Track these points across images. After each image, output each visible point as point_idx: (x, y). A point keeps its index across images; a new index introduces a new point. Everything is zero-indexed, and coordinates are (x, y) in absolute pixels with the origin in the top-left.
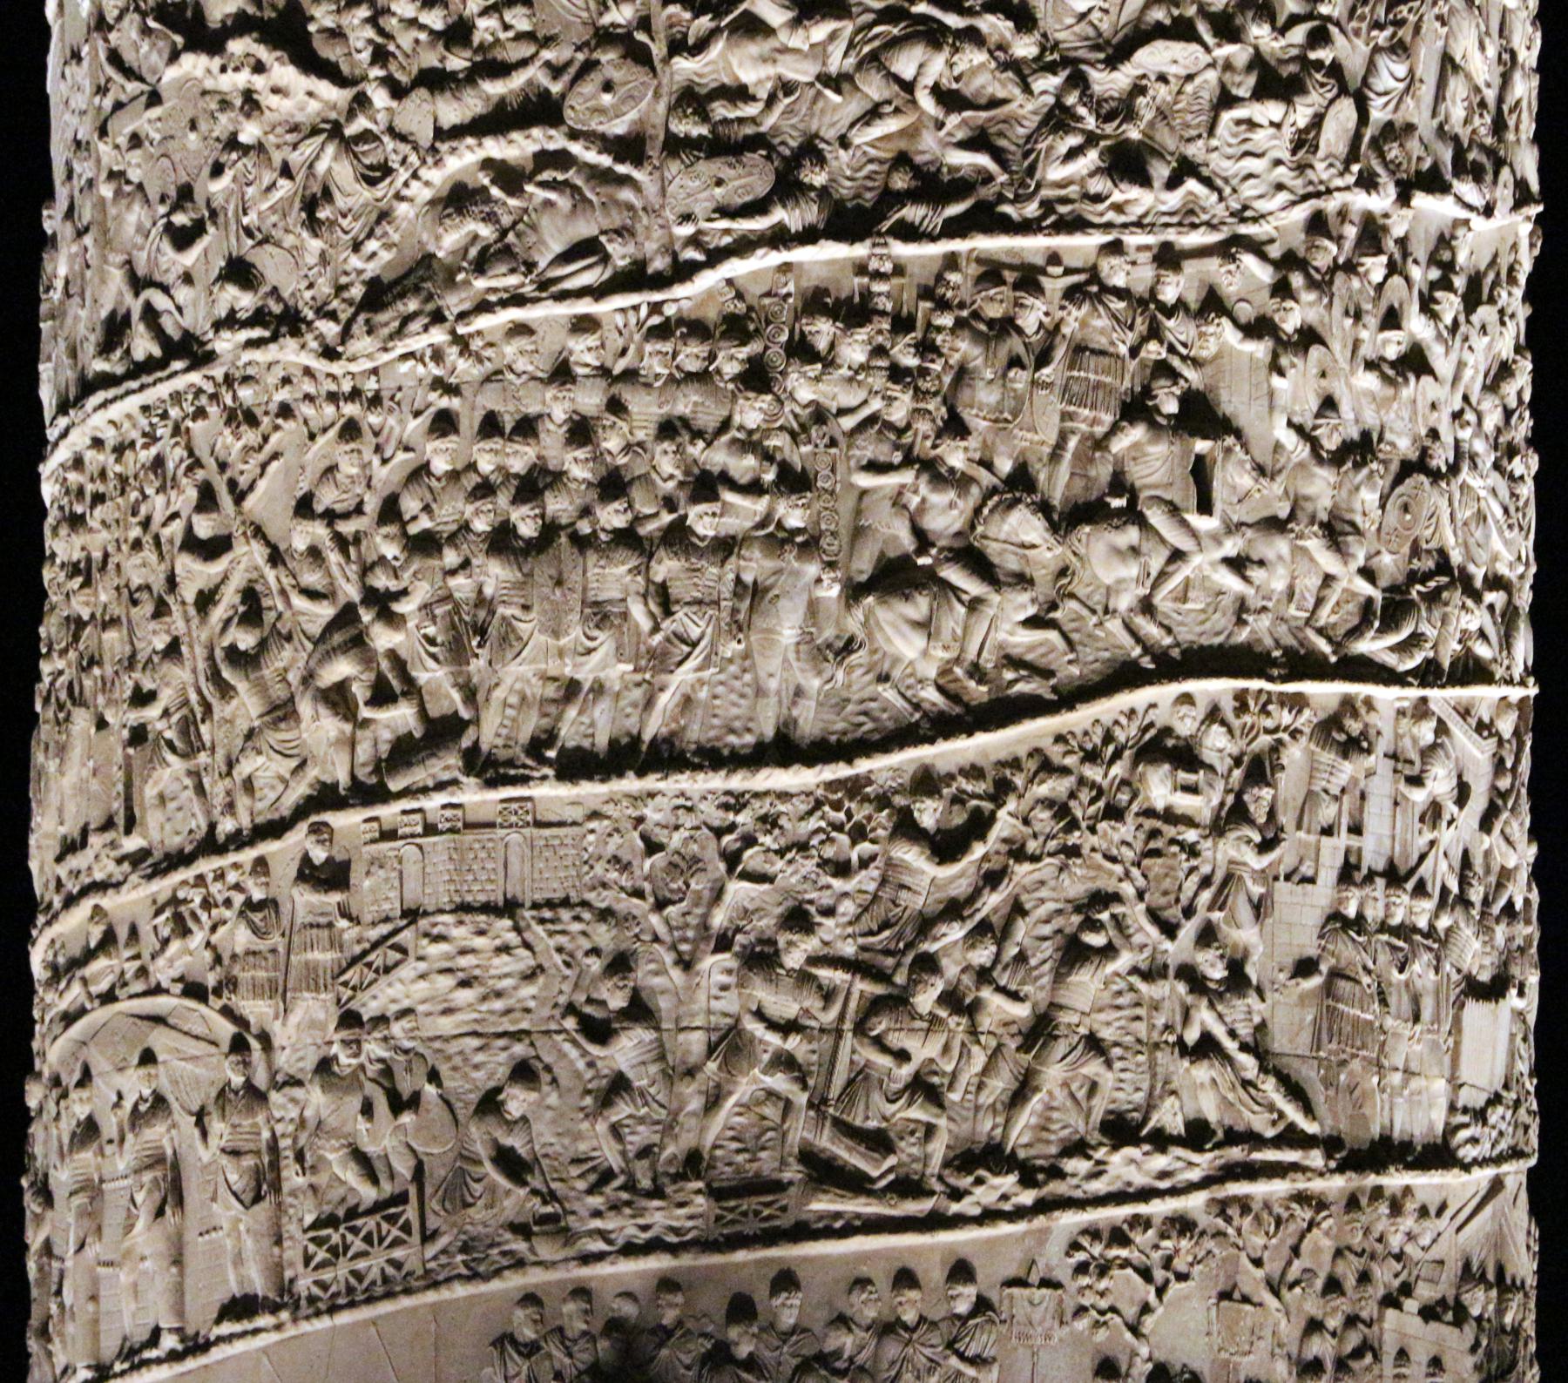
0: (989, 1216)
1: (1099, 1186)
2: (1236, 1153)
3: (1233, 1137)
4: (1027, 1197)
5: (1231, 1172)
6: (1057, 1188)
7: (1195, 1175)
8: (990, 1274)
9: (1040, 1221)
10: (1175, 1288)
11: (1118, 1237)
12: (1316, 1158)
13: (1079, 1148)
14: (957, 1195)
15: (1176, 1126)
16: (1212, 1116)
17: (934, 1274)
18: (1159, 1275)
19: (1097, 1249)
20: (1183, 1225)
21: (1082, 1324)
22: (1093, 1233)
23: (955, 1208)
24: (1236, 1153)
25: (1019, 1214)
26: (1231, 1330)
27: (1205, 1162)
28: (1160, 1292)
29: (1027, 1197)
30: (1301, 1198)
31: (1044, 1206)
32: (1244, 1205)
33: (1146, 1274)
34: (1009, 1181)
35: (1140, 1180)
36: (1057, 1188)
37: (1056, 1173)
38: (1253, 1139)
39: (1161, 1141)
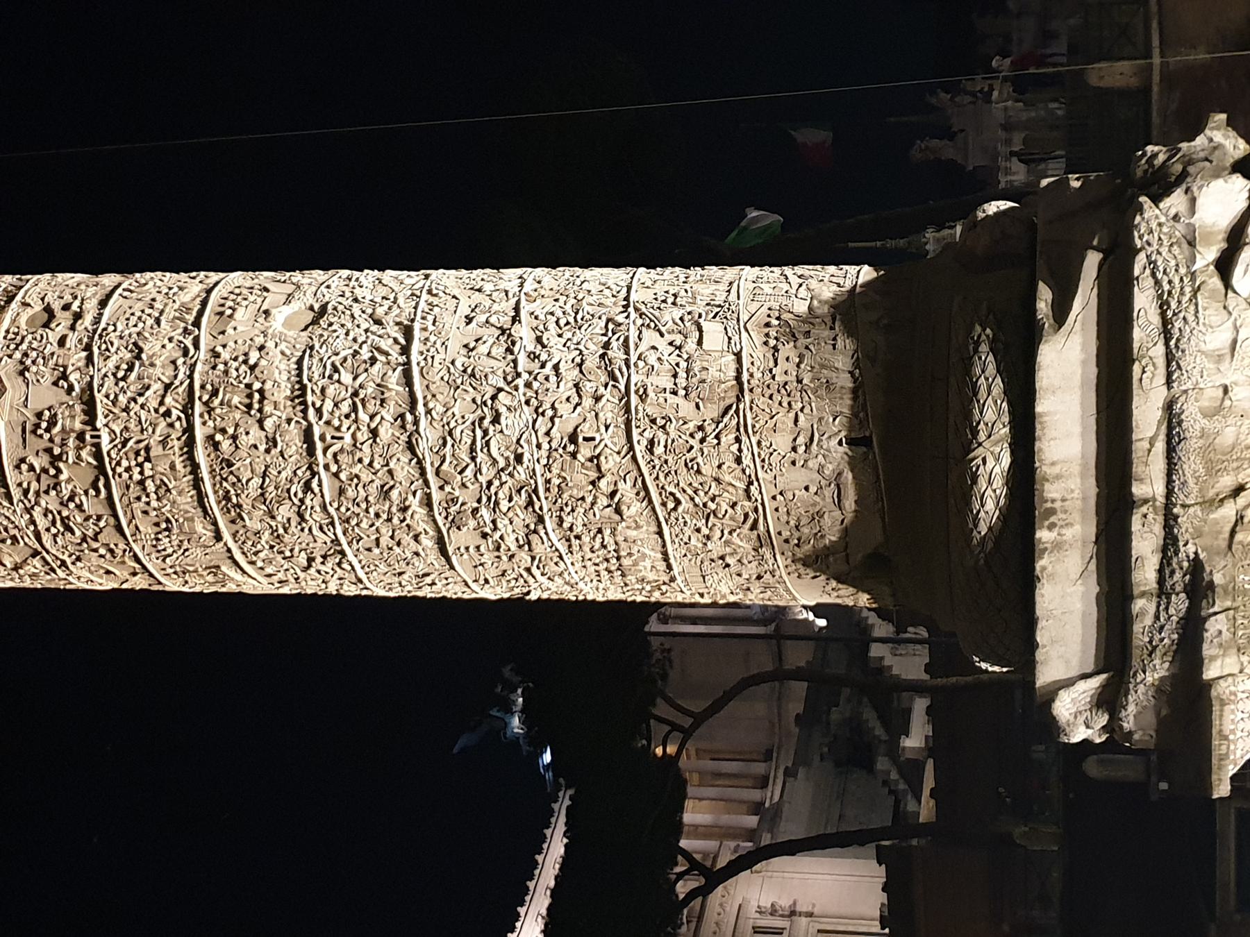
0: (761, 493)
1: (752, 466)
2: (742, 429)
3: (738, 430)
4: (756, 483)
5: (746, 431)
6: (753, 477)
7: (748, 441)
8: (774, 492)
9: (761, 481)
10: (774, 447)
11: (763, 461)
12: (741, 406)
13: (744, 471)
14: (756, 500)
15: (737, 446)
16: (734, 436)
17: (775, 504)
18: (771, 450)
19: (766, 467)
20: (759, 443)
21: (784, 470)
22: (763, 467)
23: (760, 501)
24: (742, 429)
25: (759, 485)
26: (784, 430)
27: (744, 438)
28: (775, 450)
29: (756, 483)
30: (751, 408)
31: (758, 480)
32: (754, 426)
33: (771, 454)
34: (752, 488)
35: (750, 455)
36: (753, 477)
37: (750, 476)
38: (738, 423)
39: (740, 450)
